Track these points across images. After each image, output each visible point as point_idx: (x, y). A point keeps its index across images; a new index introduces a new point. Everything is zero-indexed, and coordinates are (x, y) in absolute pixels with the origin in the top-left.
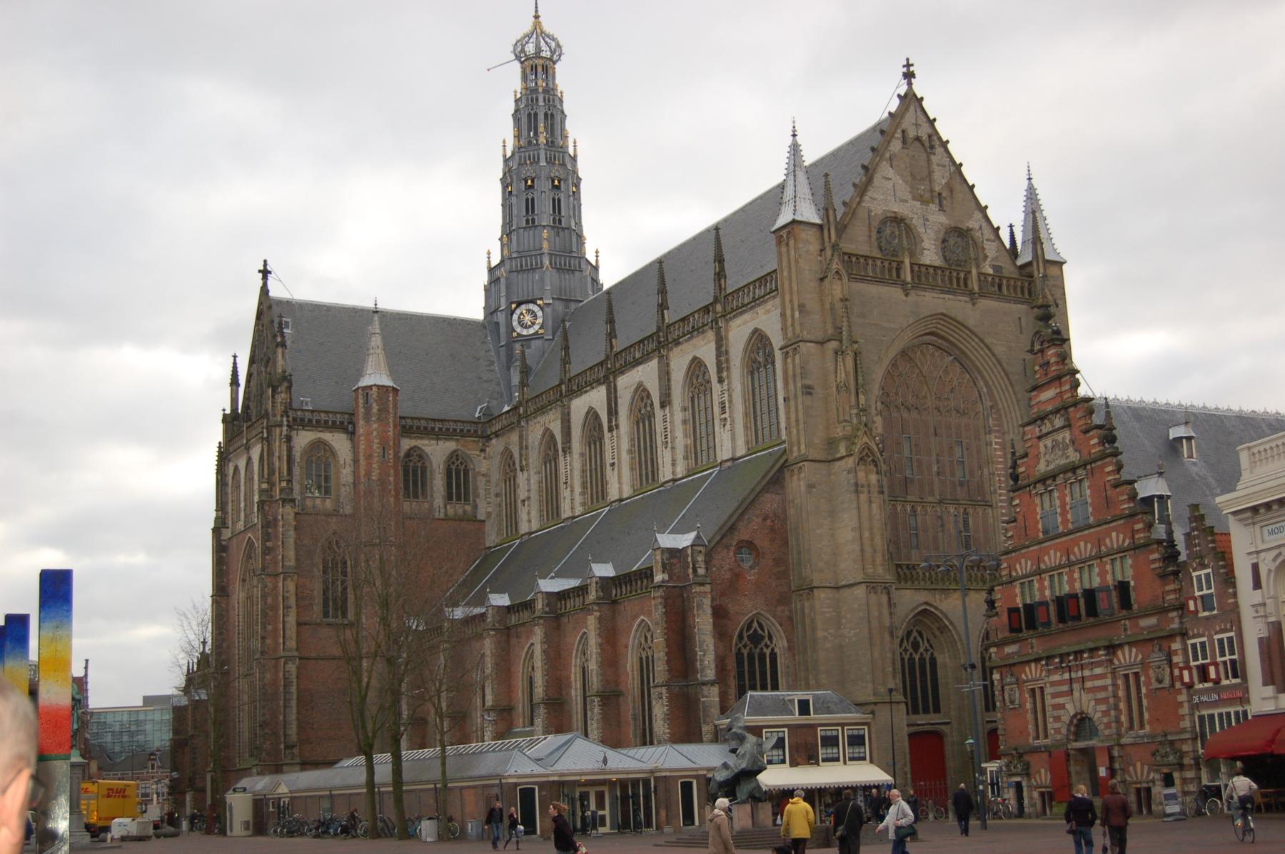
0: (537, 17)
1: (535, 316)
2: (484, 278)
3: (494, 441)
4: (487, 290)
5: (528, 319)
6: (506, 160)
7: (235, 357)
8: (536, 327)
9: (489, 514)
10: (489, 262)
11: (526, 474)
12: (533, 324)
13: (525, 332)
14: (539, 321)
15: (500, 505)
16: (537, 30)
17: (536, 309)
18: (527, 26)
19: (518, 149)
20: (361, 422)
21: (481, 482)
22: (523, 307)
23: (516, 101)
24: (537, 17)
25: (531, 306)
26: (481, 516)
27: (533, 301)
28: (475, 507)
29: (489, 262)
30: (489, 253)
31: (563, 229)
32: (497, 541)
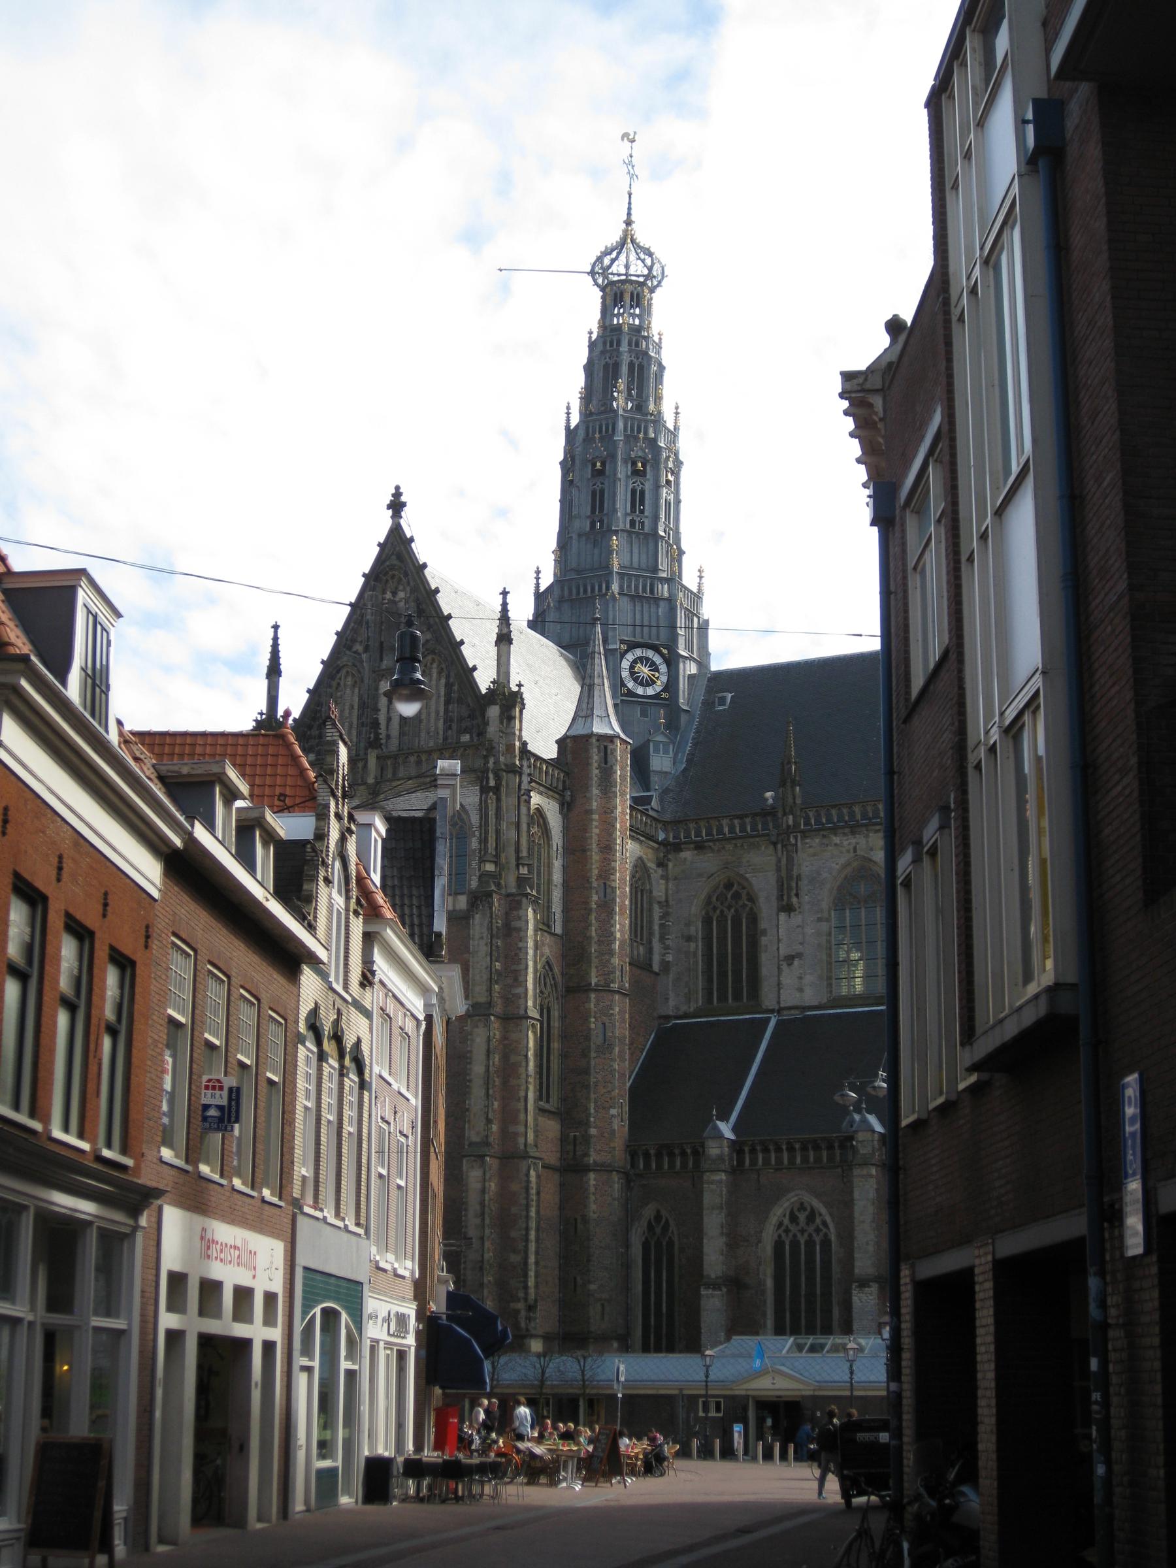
0: (629, 223)
1: (654, 668)
3: (687, 855)
5: (644, 671)
7: (276, 627)
9: (666, 966)
11: (796, 919)
13: (640, 691)
14: (664, 679)
15: (695, 954)
16: (627, 240)
17: (658, 659)
20: (595, 791)
21: (657, 911)
22: (638, 652)
24: (629, 223)
25: (650, 654)
26: (656, 967)
28: (650, 951)
32: (684, 1009)
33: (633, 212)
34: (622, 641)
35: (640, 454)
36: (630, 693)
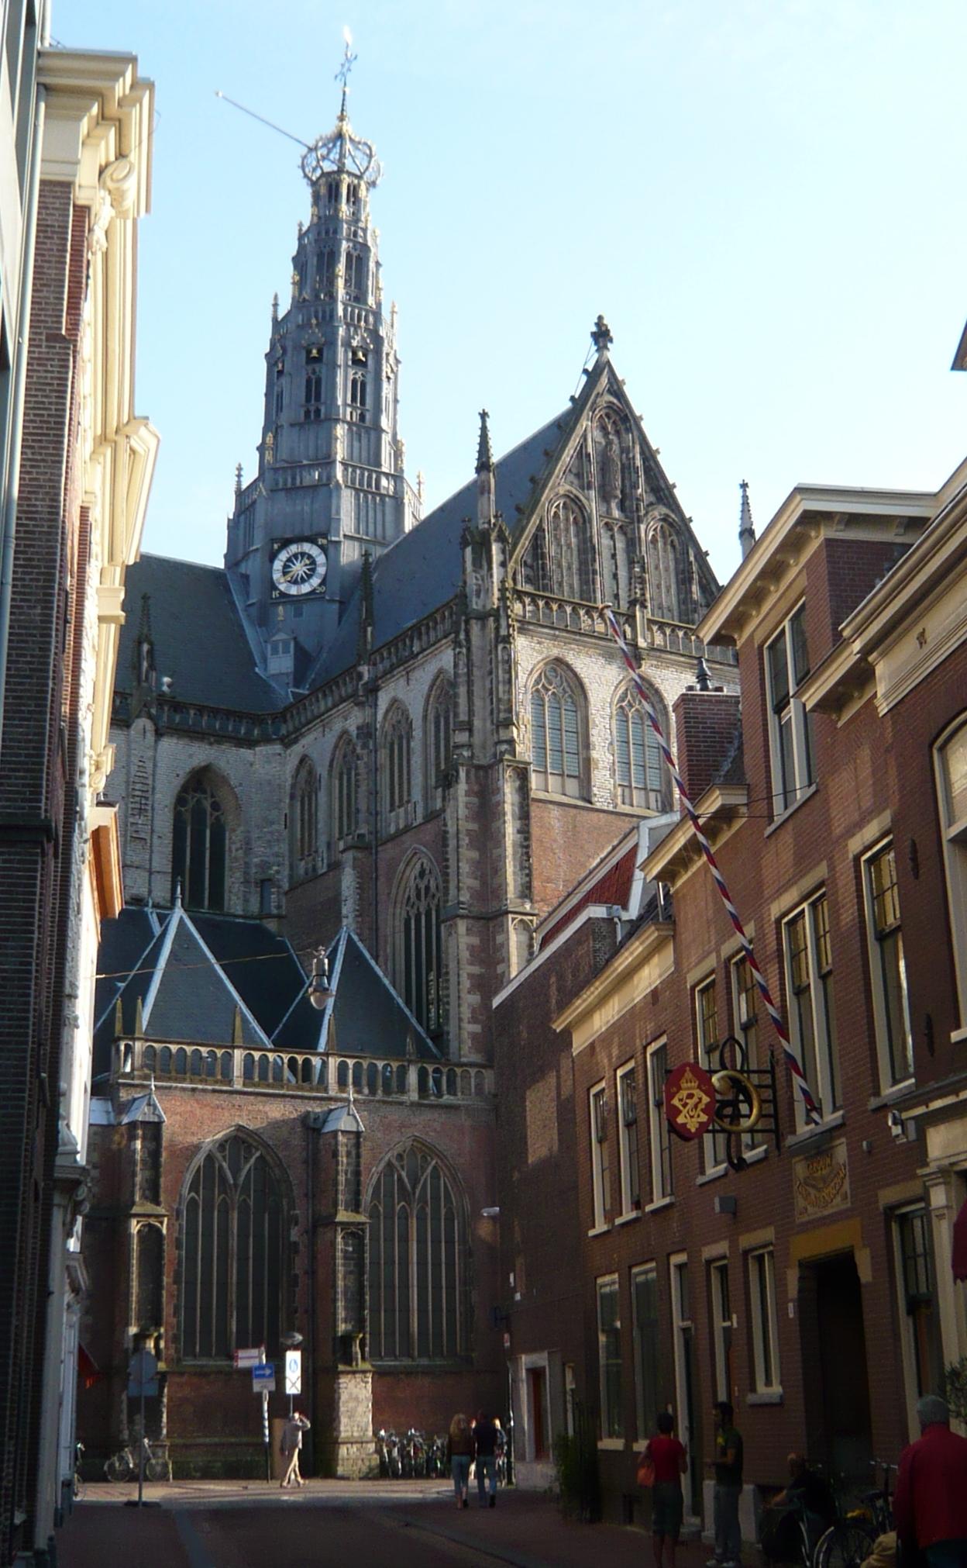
2: (229, 508)
4: (233, 526)
5: (299, 568)
6: (276, 324)
8: (315, 581)
10: (239, 483)
12: (309, 576)
13: (294, 590)
14: (321, 570)
17: (314, 551)
18: (330, 130)
19: (298, 304)
22: (294, 549)
23: (301, 237)
24: (342, 118)
25: (307, 547)
27: (312, 540)
29: (239, 483)
30: (239, 469)
31: (368, 430)
33: (347, 107)
34: (273, 541)
35: (313, 339)
36: (283, 595)
